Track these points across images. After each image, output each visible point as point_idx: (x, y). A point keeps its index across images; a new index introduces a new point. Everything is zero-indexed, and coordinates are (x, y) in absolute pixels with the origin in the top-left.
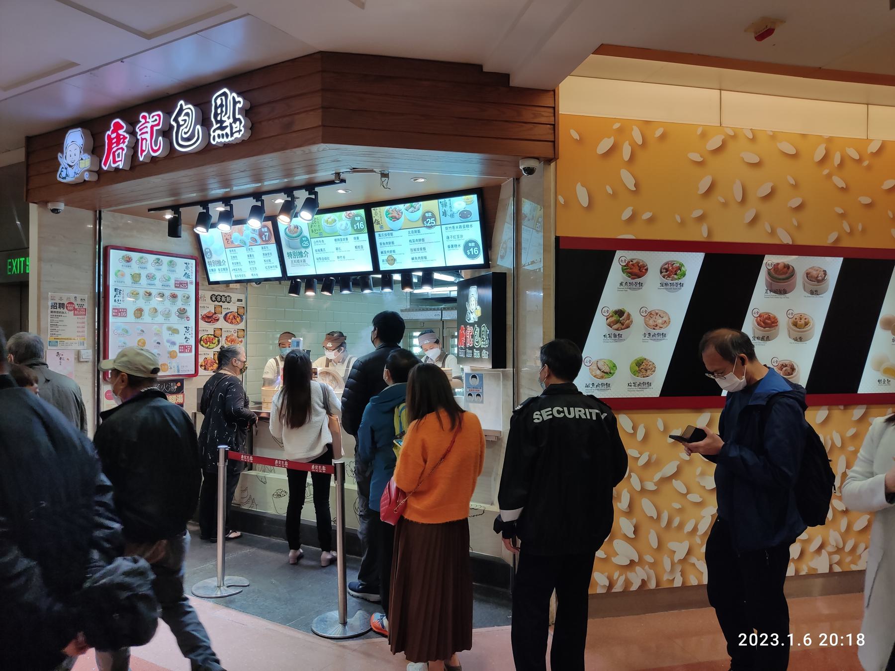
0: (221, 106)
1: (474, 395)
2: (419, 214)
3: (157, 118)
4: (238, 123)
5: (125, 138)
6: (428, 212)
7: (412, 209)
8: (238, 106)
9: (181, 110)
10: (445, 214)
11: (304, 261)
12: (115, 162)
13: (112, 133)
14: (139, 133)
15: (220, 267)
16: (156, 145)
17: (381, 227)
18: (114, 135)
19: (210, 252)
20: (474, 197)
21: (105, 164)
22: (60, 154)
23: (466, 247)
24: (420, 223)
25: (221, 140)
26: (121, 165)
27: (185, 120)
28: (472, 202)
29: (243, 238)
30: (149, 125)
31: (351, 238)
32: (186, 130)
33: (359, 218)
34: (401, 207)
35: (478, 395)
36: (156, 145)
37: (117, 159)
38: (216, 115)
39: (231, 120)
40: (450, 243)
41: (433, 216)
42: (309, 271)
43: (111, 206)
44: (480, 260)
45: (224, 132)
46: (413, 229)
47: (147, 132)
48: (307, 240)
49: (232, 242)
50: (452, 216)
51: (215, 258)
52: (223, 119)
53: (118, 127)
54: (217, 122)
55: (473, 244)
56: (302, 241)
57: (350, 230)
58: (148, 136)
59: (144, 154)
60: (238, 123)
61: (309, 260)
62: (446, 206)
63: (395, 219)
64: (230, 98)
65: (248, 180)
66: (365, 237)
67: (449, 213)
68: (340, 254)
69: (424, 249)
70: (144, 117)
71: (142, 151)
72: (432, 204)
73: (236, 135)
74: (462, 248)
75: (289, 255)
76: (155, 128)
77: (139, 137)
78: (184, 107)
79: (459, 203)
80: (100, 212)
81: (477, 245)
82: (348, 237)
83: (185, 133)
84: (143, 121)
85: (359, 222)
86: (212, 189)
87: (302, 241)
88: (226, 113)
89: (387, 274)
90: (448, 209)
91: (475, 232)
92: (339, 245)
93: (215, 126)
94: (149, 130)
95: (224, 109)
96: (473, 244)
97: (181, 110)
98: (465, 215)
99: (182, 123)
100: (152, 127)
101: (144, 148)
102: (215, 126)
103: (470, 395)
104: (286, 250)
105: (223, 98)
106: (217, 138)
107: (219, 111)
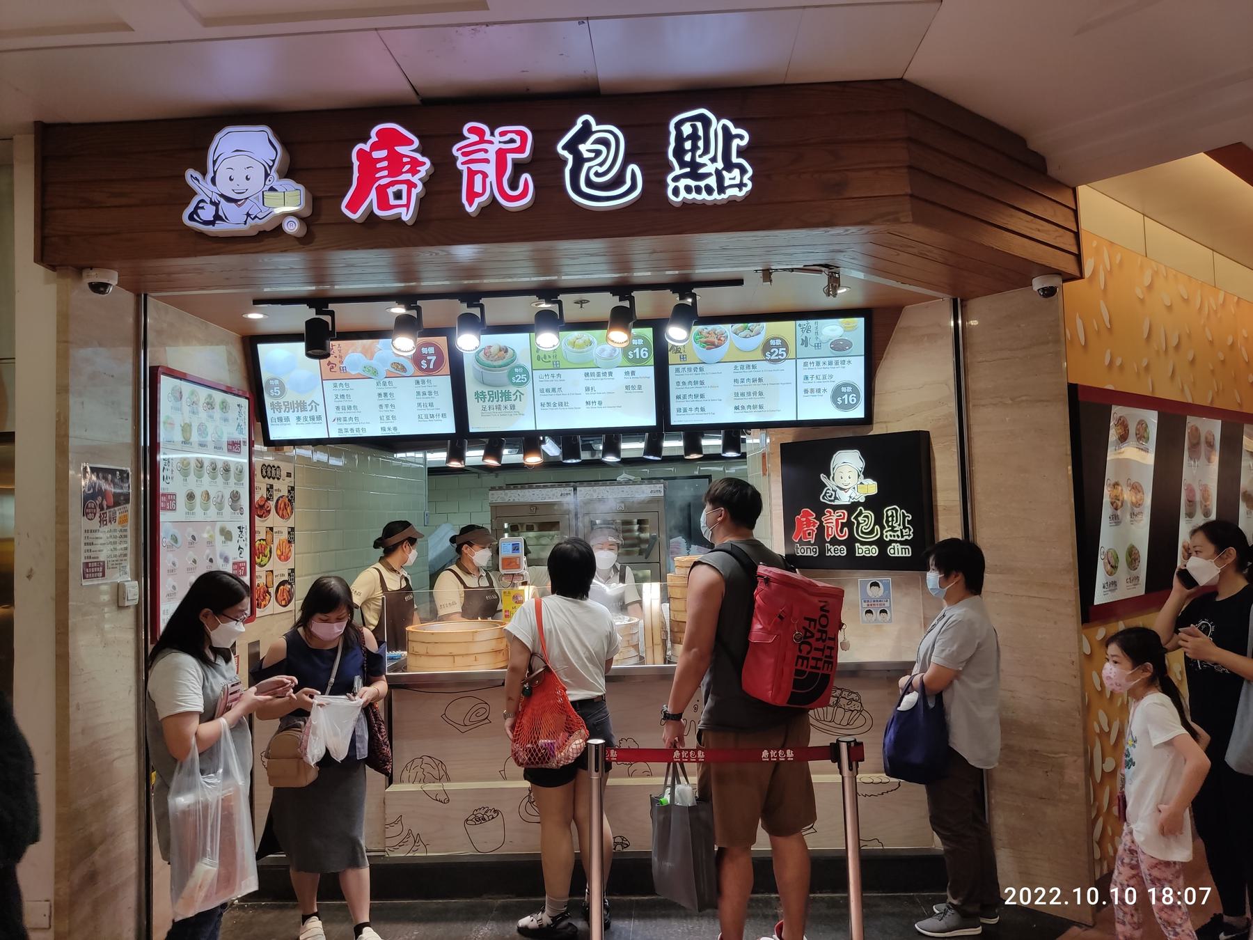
0: (694, 137)
1: (876, 613)
2: (759, 341)
3: (517, 138)
4: (736, 172)
5: (415, 164)
6: (774, 338)
7: (747, 332)
8: (736, 143)
9: (586, 132)
10: (805, 342)
11: (513, 407)
12: (384, 203)
13: (375, 147)
14: (461, 159)
15: (302, 414)
16: (514, 186)
17: (683, 358)
18: (383, 153)
19: (282, 386)
20: (860, 322)
21: (353, 206)
22: (190, 173)
23: (837, 393)
24: (759, 355)
25: (694, 195)
26: (407, 215)
27: (598, 153)
28: (855, 328)
29: (374, 363)
30: (492, 150)
31: (619, 373)
32: (601, 170)
33: (640, 342)
34: (726, 328)
35: (883, 611)
36: (514, 186)
37: (392, 202)
38: (679, 152)
39: (720, 165)
40: (809, 386)
41: (784, 344)
42: (525, 424)
43: (161, 290)
44: (859, 413)
45: (702, 184)
46: (741, 361)
47: (487, 161)
48: (525, 371)
49: (343, 369)
50: (818, 346)
51: (291, 396)
52: (698, 160)
53: (389, 140)
54: (683, 164)
55: (849, 389)
56: (512, 374)
57: (620, 359)
58: (491, 169)
59: (477, 201)
60: (736, 172)
61: (525, 405)
62: (808, 330)
63: (711, 345)
64: (717, 125)
65: (604, 267)
66: (649, 372)
67: (812, 341)
68: (590, 398)
69: (761, 394)
70: (480, 133)
71: (472, 195)
72: (785, 329)
73: (731, 192)
74: (829, 393)
75: (479, 396)
76: (510, 157)
77: (464, 168)
78: (595, 127)
79: (832, 329)
80: (146, 296)
81: (855, 390)
82: (615, 371)
83: (597, 174)
85: (640, 347)
86: (427, 279)
87: (512, 374)
88: (706, 151)
89: (693, 434)
90: (811, 335)
91: (854, 371)
92: (590, 383)
93: (678, 171)
94: (492, 156)
95: (701, 144)
96: (849, 389)
97: (586, 132)
98: (839, 346)
99: (586, 155)
100: (501, 154)
101: (478, 188)
103: (869, 612)
104: (471, 388)
105: (699, 125)
106: (679, 189)
107: (688, 145)
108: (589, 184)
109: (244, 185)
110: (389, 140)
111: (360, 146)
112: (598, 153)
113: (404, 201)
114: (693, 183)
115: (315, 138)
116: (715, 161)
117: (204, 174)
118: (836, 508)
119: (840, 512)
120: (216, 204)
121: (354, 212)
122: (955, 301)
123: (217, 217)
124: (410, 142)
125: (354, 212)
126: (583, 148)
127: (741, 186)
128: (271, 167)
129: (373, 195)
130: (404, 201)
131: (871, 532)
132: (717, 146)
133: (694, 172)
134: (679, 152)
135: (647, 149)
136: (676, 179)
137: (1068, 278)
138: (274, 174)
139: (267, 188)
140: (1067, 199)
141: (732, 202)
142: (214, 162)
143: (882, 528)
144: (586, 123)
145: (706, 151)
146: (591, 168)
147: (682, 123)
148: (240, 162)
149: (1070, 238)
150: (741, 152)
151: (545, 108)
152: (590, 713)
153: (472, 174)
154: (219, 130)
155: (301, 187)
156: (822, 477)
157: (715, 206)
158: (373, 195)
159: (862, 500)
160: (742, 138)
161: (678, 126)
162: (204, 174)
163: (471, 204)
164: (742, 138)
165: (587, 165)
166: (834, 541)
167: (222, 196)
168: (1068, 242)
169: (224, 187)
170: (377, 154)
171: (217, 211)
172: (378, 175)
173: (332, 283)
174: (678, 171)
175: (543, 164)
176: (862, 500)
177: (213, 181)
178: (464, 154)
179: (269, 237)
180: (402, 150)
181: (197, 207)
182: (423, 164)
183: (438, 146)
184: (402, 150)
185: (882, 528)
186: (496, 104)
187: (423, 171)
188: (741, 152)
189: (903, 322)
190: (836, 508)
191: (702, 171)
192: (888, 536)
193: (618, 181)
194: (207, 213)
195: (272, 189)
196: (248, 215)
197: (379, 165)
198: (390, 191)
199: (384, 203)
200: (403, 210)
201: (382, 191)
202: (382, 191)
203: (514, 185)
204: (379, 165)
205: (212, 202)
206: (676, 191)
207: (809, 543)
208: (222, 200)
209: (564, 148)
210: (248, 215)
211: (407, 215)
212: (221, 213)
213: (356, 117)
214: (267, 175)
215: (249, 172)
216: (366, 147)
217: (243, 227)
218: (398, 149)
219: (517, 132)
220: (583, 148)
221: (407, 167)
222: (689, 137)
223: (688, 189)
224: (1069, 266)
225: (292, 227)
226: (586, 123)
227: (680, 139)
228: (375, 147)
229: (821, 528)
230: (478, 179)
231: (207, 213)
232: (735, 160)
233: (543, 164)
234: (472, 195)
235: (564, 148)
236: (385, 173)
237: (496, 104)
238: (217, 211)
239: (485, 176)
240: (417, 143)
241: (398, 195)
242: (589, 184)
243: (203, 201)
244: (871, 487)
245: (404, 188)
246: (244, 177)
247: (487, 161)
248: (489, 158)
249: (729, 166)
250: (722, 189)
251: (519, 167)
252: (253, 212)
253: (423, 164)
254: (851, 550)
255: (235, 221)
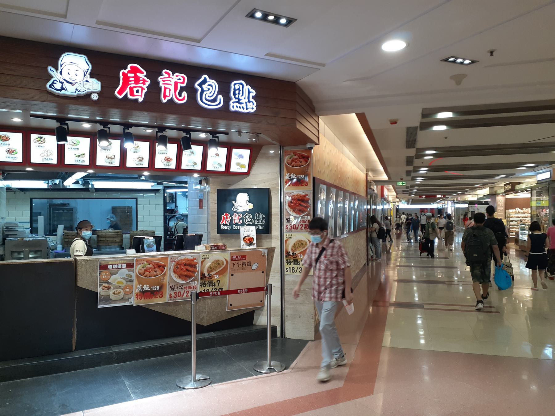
0: (239, 89)
3: (182, 79)
5: (144, 81)
8: (251, 95)
12: (132, 94)
14: (161, 83)
16: (180, 95)
18: (132, 75)
21: (120, 93)
26: (141, 100)
32: (210, 95)
37: (135, 93)
38: (234, 94)
39: (247, 101)
45: (241, 106)
54: (236, 98)
58: (172, 88)
59: (167, 99)
60: (251, 103)
70: (169, 74)
76: (179, 85)
77: (163, 86)
84: (167, 76)
88: (242, 95)
94: (173, 84)
97: (205, 81)
99: (205, 89)
100: (176, 84)
101: (167, 94)
102: (234, 100)
106: (234, 106)
107: (237, 92)
108: (206, 99)
109: (74, 77)
110: (134, 70)
111: (123, 71)
112: (209, 89)
113: (140, 94)
114: (238, 105)
115: (105, 64)
116: (245, 100)
117: (57, 69)
118: (237, 213)
119: (239, 214)
120: (62, 83)
121: (120, 95)
122: (281, 147)
123: (62, 88)
124: (143, 73)
125: (120, 95)
126: (204, 86)
127: (252, 108)
128: (87, 72)
129: (128, 90)
130: (140, 94)
131: (251, 221)
132: (246, 94)
133: (239, 102)
134: (234, 94)
135: (224, 90)
136: (233, 103)
137: (316, 144)
138: (88, 75)
139: (85, 80)
140: (316, 118)
141: (249, 113)
142: (61, 66)
143: (255, 220)
144: (205, 78)
145: (242, 95)
146: (207, 94)
147: (235, 85)
148: (73, 68)
149: (317, 133)
150: (253, 97)
151: (193, 71)
152: (205, 279)
153: (165, 88)
154: (64, 52)
155: (100, 83)
156: (233, 202)
157: (243, 113)
158: (128, 90)
159: (248, 210)
160: (253, 93)
161: (235, 85)
162: (57, 69)
163: (165, 99)
164: (253, 93)
165: (205, 93)
166: (237, 224)
167: (64, 80)
168: (317, 134)
169: (65, 76)
170: (130, 75)
171: (62, 85)
172: (130, 83)
173: (68, 114)
174: (234, 100)
175: (190, 89)
176: (248, 210)
177: (61, 73)
178: (163, 81)
179: (84, 99)
180: (139, 74)
181: (53, 83)
182: (147, 82)
183: (154, 75)
184: (139, 74)
185: (255, 220)
186: (176, 66)
187: (147, 84)
188: (253, 97)
189: (262, 151)
190: (237, 213)
191: (241, 101)
192: (256, 223)
193: (215, 100)
194: (58, 86)
195: (87, 81)
196: (76, 90)
197: (131, 79)
198: (135, 90)
199: (132, 94)
200: (139, 98)
201: (131, 89)
202: (131, 89)
203: (180, 95)
204: (131, 79)
205: (60, 82)
206: (233, 107)
207: (227, 225)
208: (65, 82)
209: (198, 85)
210: (76, 90)
211: (141, 100)
212: (64, 87)
213: (124, 59)
214: (85, 75)
215: (77, 72)
216: (126, 71)
217: (74, 94)
218: (138, 74)
219: (183, 77)
220: (204, 86)
221: (142, 82)
222: (238, 89)
223: (237, 107)
224: (315, 140)
225: (95, 97)
226: (205, 78)
227: (235, 90)
228: (129, 72)
229: (232, 220)
230: (168, 90)
231: (58, 86)
232: (251, 99)
233: (190, 89)
234: (165, 96)
235: (198, 85)
236: (133, 82)
237: (176, 66)
238: (62, 85)
239: (170, 90)
240: (145, 73)
241: (137, 92)
242: (206, 99)
243: (56, 80)
244: (251, 206)
245: (140, 89)
246: (73, 74)
247: (171, 85)
248: (171, 84)
249: (249, 102)
250: (247, 109)
251: (182, 89)
252: (79, 89)
253: (147, 82)
254: (232, 228)
255: (70, 91)
